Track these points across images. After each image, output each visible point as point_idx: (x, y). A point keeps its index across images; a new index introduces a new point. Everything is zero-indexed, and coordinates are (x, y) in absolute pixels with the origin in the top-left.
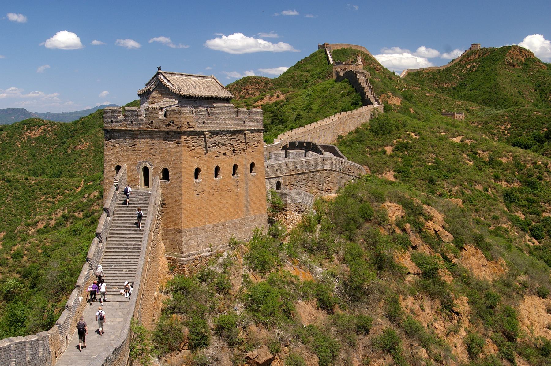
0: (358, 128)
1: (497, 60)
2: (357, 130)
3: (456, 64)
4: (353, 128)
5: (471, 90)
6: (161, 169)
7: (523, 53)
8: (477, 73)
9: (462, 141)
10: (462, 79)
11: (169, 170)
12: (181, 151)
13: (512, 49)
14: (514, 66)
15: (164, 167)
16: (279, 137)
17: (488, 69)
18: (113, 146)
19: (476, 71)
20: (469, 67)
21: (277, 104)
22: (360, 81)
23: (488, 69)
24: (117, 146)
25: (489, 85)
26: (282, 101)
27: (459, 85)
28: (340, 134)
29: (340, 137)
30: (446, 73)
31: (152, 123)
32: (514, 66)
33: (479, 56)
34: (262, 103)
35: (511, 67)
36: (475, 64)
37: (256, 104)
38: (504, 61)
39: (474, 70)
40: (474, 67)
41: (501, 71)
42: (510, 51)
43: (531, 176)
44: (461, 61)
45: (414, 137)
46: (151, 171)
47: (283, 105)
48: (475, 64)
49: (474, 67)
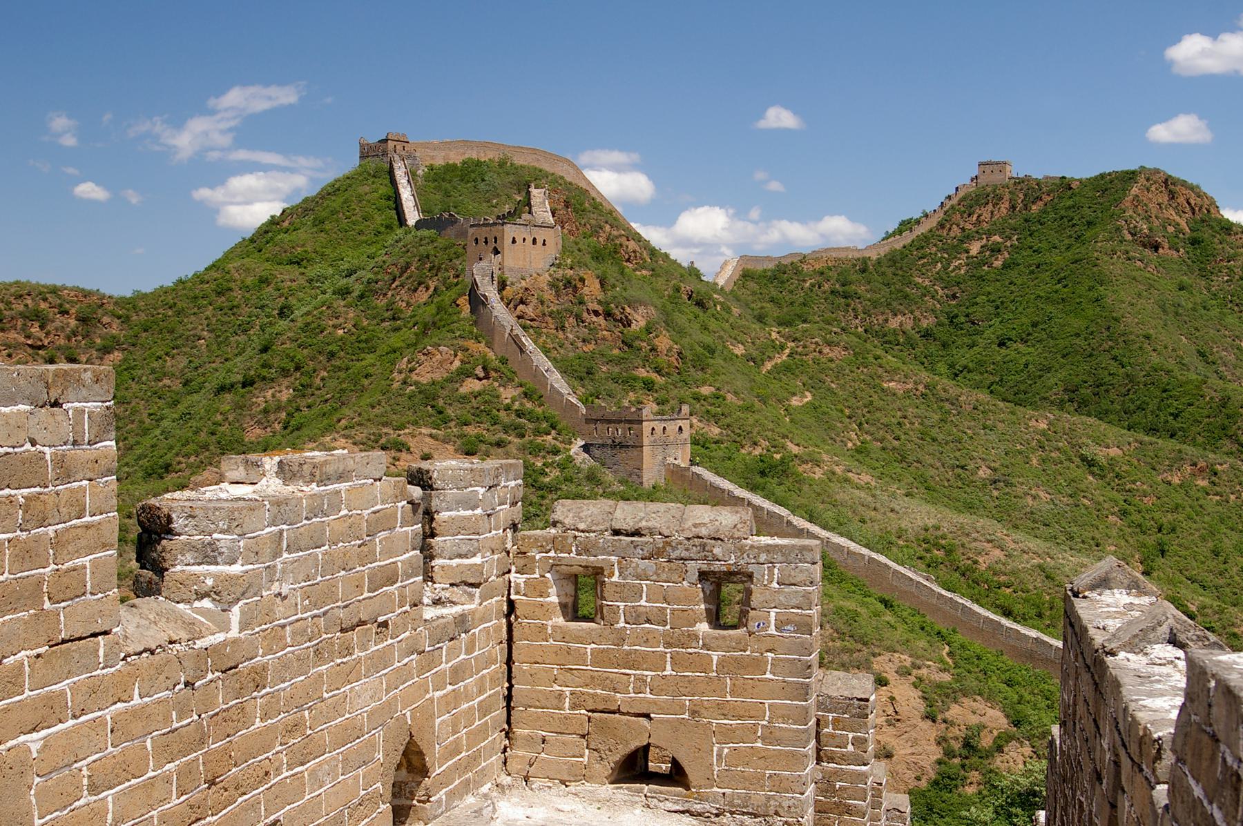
1: (1090, 224)
3: (925, 240)
5: (1002, 344)
7: (1181, 200)
8: (1013, 274)
10: (954, 297)
13: (1142, 180)
14: (1156, 247)
17: (1056, 258)
19: (1006, 266)
20: (975, 248)
23: (1056, 258)
25: (1077, 323)
27: (943, 319)
30: (889, 271)
32: (1156, 247)
33: (1013, 207)
35: (1148, 252)
36: (997, 238)
38: (1118, 229)
39: (998, 263)
40: (996, 250)
41: (1114, 267)
42: (1135, 190)
44: (941, 226)
48: (997, 238)
49: (996, 250)
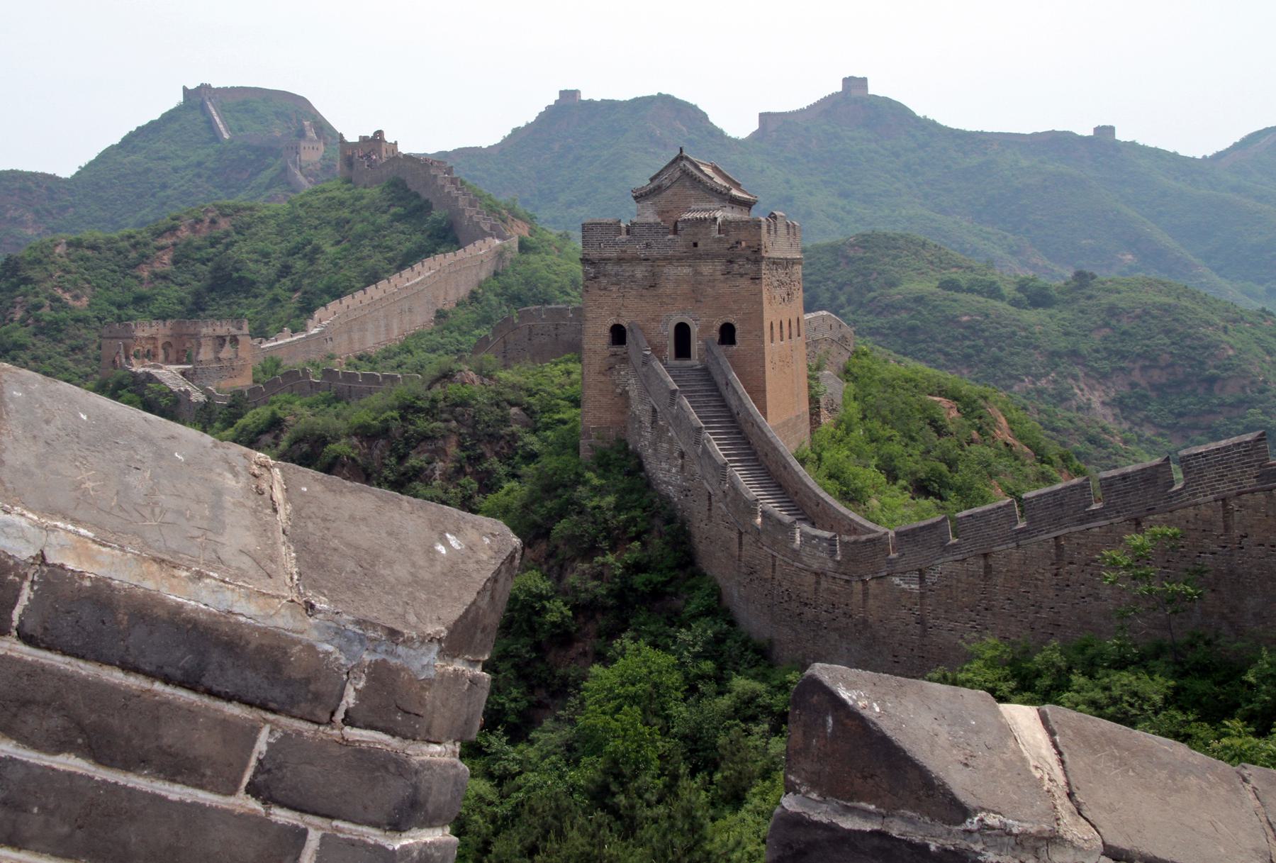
0: (473, 293)
2: (473, 296)
4: (463, 292)
6: (718, 324)
11: (737, 326)
12: (761, 292)
15: (726, 320)
16: (317, 315)
18: (605, 289)
21: (214, 242)
22: (440, 182)
24: (614, 288)
26: (227, 234)
28: (440, 306)
29: (441, 315)
31: (695, 245)
34: (174, 239)
37: (163, 242)
46: (695, 330)
47: (232, 244)
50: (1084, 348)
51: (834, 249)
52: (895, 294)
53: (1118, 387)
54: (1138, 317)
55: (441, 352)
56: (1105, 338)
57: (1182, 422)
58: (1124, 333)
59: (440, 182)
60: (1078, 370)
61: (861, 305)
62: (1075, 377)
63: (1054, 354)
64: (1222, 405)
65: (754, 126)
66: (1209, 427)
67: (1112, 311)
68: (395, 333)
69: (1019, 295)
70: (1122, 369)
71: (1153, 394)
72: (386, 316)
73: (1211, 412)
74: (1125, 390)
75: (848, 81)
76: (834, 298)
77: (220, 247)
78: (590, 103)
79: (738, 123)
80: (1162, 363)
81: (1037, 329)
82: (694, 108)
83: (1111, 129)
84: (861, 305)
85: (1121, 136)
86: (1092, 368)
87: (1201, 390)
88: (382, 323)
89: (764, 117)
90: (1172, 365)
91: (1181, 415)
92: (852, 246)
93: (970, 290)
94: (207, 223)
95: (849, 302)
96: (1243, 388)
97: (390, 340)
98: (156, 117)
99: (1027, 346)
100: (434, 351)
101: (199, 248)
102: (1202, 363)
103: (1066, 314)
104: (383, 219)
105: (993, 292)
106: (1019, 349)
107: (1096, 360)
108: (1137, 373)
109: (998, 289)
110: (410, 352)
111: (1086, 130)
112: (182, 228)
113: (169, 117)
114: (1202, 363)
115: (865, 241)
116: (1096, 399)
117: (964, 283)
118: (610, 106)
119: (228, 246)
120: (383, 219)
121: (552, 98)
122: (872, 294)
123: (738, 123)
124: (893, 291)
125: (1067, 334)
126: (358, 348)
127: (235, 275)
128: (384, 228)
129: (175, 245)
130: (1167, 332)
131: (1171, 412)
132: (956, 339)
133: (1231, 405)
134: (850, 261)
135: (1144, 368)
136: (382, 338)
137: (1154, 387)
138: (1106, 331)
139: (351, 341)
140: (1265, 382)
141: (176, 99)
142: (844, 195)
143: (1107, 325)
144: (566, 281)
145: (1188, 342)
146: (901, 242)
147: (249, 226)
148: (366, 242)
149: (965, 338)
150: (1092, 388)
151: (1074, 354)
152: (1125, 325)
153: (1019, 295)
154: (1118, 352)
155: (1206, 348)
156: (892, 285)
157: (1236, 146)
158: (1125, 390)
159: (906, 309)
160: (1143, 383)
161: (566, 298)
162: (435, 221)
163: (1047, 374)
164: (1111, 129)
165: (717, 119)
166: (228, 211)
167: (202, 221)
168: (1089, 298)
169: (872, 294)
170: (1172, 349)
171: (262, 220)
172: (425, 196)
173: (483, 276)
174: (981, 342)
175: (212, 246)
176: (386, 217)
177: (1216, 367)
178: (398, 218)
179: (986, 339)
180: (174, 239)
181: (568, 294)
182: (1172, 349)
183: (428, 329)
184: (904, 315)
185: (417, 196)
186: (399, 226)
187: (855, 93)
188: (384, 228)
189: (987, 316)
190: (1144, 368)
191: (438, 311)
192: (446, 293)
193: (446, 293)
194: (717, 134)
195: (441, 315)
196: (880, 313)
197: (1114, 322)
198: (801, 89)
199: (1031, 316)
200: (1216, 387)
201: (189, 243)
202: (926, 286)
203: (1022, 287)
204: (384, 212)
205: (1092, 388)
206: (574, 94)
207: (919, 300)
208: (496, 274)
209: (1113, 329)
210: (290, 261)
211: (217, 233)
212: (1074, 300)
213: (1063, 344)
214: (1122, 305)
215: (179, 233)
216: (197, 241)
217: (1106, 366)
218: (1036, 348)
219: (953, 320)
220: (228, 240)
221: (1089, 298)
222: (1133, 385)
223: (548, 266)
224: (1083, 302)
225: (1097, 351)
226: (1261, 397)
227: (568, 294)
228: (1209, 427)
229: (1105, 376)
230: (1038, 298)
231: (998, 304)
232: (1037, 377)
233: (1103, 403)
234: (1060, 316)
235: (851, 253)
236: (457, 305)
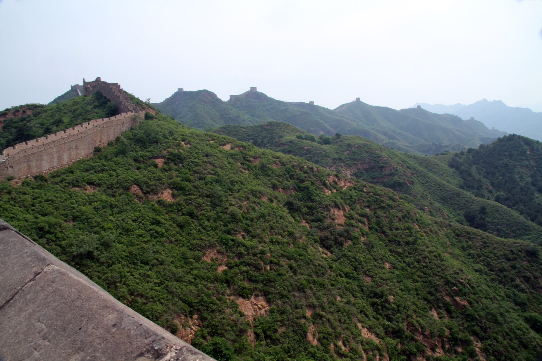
2: (118, 139)
4: (112, 138)
9: (232, 148)
26: (29, 116)
29: (97, 150)
34: (5, 119)
43: (302, 181)
45: (185, 146)
47: (30, 120)
50: (343, 157)
51: (261, 126)
52: (283, 140)
53: (354, 170)
54: (357, 147)
55: (92, 171)
56: (348, 154)
57: (374, 181)
58: (354, 152)
59: (113, 91)
60: (342, 164)
61: (272, 143)
62: (341, 167)
63: (334, 159)
64: (386, 175)
65: (229, 98)
66: (382, 182)
67: (349, 145)
68: (66, 160)
69: (321, 141)
70: (355, 164)
71: (364, 172)
72: (58, 152)
73: (383, 177)
74: (356, 170)
75: (252, 88)
76: (262, 142)
77: (25, 122)
78: (186, 92)
79: (224, 97)
80: (366, 162)
81: (328, 151)
82: (213, 93)
83: (313, 102)
84: (272, 143)
85: (315, 104)
86: (346, 164)
87: (378, 171)
88: (55, 156)
89: (232, 97)
90: (370, 163)
91: (373, 178)
92: (267, 125)
93: (306, 139)
94: (21, 113)
95: (268, 142)
96: (391, 170)
97: (62, 165)
98: (63, 94)
99: (326, 156)
100: (87, 170)
101: (15, 122)
102: (378, 162)
103: (335, 146)
104: (89, 108)
105: (312, 139)
106: (324, 158)
107: (347, 161)
108: (359, 165)
109: (314, 139)
110: (72, 172)
111: (307, 102)
112: (9, 114)
113: (67, 93)
114: (378, 162)
115: (271, 124)
116: (348, 173)
117: (304, 137)
118: (191, 93)
119: (28, 122)
120: (89, 108)
121: (176, 90)
122: (275, 140)
123: (224, 97)
124: (282, 139)
125: (337, 153)
126: (35, 171)
127: (26, 133)
128: (89, 111)
129: (5, 121)
130: (367, 152)
131: (371, 177)
132: (304, 154)
133: (388, 175)
134: (266, 130)
135: (361, 164)
136: (55, 164)
137: (364, 169)
138: (348, 152)
139: (29, 167)
140: (396, 168)
141: (69, 89)
142: (252, 116)
143: (348, 150)
144: (167, 132)
145: (373, 155)
146: (281, 124)
147: (39, 113)
148: (81, 117)
149: (307, 154)
150: (347, 170)
151: (340, 159)
152: (354, 150)
153: (321, 141)
154: (353, 159)
155: (379, 157)
156: (282, 137)
157: (338, 108)
158: (356, 170)
159: (287, 145)
160: (362, 168)
161: (166, 140)
162: (110, 107)
163: (333, 166)
164: (313, 102)
165: (219, 96)
166: (31, 107)
167: (19, 111)
168: (341, 141)
169: (275, 140)
170: (369, 157)
171: (46, 111)
172: (108, 97)
173: (124, 129)
174: (312, 155)
175: (22, 121)
176: (92, 106)
177: (383, 163)
178: (95, 107)
179: (313, 154)
180: (5, 119)
181: (167, 138)
182: (369, 157)
183: (88, 158)
184: (286, 147)
185: (105, 98)
186: (96, 110)
187: (254, 91)
188: (89, 111)
189: (313, 147)
190: (361, 164)
191: (95, 148)
192: (101, 138)
193: (101, 138)
194: (219, 100)
195: (97, 150)
196: (278, 146)
197: (350, 149)
198: (240, 90)
199: (325, 147)
200: (383, 169)
201: (11, 120)
202: (293, 138)
203: (321, 138)
204: (91, 105)
205: (347, 170)
206: (182, 89)
207: (291, 142)
208: (131, 129)
209: (350, 151)
210: (50, 127)
211: (25, 116)
212: (337, 142)
213: (336, 156)
214: (352, 144)
215: (7, 116)
216: (15, 119)
217: (350, 163)
218: (329, 157)
219: (302, 148)
220: (29, 119)
221: (341, 141)
222: (359, 169)
223: (158, 125)
224: (340, 143)
225: (346, 158)
226: (396, 173)
227: (167, 138)
228: (382, 182)
229: (350, 166)
230: (326, 142)
231: (313, 143)
232: (330, 167)
233: (351, 175)
234: (334, 147)
235: (266, 128)
236: (108, 144)
